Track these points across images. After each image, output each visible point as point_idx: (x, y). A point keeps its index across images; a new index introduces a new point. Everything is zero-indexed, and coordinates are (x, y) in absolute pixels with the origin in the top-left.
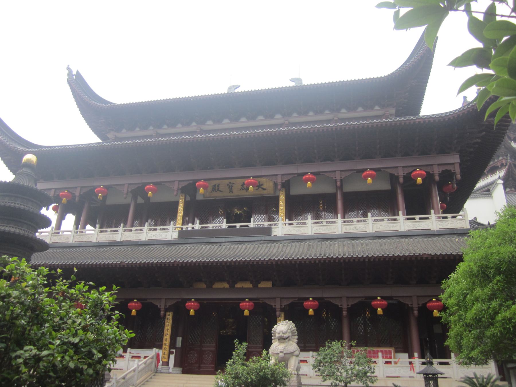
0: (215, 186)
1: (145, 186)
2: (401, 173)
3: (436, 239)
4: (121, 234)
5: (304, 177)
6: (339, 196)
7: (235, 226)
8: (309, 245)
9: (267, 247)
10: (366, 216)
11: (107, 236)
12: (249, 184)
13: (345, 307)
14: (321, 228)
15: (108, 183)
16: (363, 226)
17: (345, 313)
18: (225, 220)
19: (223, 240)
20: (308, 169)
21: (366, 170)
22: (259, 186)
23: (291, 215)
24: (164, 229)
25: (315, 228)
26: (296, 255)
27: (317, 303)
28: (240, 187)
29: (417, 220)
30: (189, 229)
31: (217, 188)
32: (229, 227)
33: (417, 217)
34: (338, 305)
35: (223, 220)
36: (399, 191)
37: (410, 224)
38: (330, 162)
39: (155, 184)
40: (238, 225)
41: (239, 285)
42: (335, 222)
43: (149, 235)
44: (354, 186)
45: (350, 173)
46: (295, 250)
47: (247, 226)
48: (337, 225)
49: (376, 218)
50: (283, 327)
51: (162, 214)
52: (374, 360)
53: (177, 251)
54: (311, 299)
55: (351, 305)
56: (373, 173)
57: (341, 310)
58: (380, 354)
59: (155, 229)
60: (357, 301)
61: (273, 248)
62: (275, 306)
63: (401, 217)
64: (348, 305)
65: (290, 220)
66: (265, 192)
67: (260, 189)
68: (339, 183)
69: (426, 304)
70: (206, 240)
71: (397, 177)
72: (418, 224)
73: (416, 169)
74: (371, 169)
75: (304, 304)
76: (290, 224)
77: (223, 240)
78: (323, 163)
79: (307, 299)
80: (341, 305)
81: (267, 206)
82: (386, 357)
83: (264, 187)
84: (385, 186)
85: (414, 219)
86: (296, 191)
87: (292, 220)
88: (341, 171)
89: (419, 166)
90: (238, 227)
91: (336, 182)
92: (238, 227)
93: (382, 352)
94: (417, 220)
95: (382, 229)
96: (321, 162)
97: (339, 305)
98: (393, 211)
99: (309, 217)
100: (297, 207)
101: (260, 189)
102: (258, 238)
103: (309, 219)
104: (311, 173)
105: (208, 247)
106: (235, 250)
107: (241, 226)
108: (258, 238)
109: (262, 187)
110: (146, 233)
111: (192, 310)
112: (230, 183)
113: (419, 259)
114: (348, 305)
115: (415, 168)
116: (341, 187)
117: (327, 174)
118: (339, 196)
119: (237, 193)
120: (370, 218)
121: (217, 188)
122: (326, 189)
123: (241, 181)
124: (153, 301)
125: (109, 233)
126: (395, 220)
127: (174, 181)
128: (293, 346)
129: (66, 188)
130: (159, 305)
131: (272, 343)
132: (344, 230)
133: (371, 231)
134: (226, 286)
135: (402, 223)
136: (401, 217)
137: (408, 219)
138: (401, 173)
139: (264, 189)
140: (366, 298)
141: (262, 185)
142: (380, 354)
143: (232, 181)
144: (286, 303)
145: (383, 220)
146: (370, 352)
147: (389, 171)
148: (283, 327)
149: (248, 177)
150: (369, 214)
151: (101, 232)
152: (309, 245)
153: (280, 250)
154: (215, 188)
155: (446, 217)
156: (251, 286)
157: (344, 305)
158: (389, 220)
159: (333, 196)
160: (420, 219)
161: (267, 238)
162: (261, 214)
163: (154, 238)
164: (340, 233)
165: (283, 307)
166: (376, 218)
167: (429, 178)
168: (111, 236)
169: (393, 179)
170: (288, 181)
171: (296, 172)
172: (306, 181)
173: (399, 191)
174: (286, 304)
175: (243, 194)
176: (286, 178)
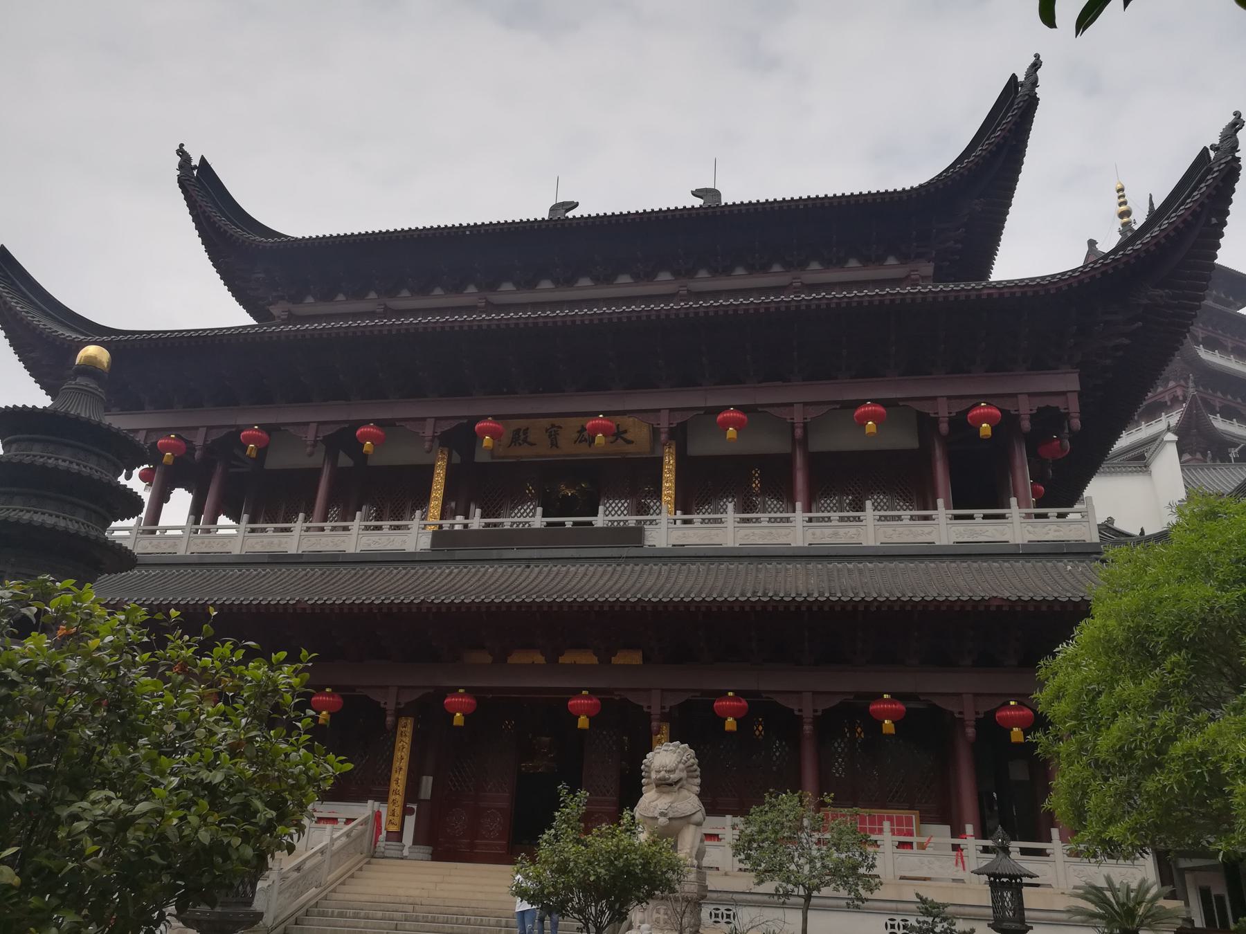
0: (517, 431)
2: (944, 412)
4: (298, 538)
5: (720, 417)
6: (799, 461)
7: (563, 524)
9: (633, 571)
10: (861, 508)
11: (266, 540)
13: (808, 714)
14: (756, 531)
15: (270, 418)
16: (853, 531)
17: (807, 728)
18: (539, 510)
19: (535, 553)
20: (729, 399)
22: (618, 434)
23: (685, 503)
24: (398, 528)
25: (742, 532)
26: (700, 592)
27: (744, 703)
29: (979, 520)
30: (457, 527)
31: (522, 437)
32: (549, 524)
33: (979, 513)
34: (792, 710)
35: (535, 508)
36: (938, 453)
37: (961, 528)
38: (780, 383)
39: (379, 423)
40: (569, 521)
41: (566, 659)
42: (788, 520)
43: (364, 539)
44: (836, 440)
45: (825, 409)
47: (590, 523)
48: (797, 529)
49: (883, 513)
50: (666, 757)
51: (396, 494)
52: (873, 837)
54: (730, 694)
55: (823, 711)
56: (880, 409)
57: (799, 721)
58: (886, 825)
59: (379, 528)
60: (836, 701)
61: (646, 574)
62: (649, 707)
63: (942, 512)
64: (815, 711)
66: (630, 448)
67: (620, 441)
68: (799, 432)
70: (494, 554)
71: (936, 421)
72: (981, 530)
73: (978, 404)
74: (875, 402)
76: (685, 522)
77: (535, 553)
78: (764, 384)
79: (722, 694)
80: (800, 710)
81: (637, 483)
82: (900, 833)
83: (628, 436)
84: (905, 440)
85: (971, 517)
86: (701, 446)
88: (805, 404)
89: (984, 397)
90: (569, 525)
92: (569, 525)
93: (890, 819)
97: (796, 708)
98: (922, 499)
99: (731, 506)
101: (620, 441)
104: (737, 408)
105: (500, 570)
107: (575, 524)
109: (625, 436)
110: (358, 537)
112: (553, 426)
113: (982, 608)
114: (815, 711)
116: (804, 441)
117: (771, 410)
118: (799, 461)
119: (568, 448)
120: (870, 512)
121: (522, 437)
122: (770, 444)
123: (575, 423)
125: (270, 533)
126: (926, 518)
127: (424, 419)
128: (688, 801)
129: (171, 430)
133: (871, 543)
134: (539, 659)
135: (944, 528)
136: (942, 512)
137: (957, 517)
138: (944, 412)
141: (625, 432)
142: (886, 825)
143: (557, 421)
144: (672, 701)
145: (899, 518)
146: (863, 821)
147: (917, 406)
148: (666, 757)
150: (868, 504)
151: (253, 531)
154: (519, 437)
155: (1045, 516)
156: (594, 660)
157: (808, 710)
158: (912, 518)
160: (985, 517)
164: (800, 544)
166: (883, 513)
167: (1006, 425)
168: (276, 540)
169: (926, 425)
170: (683, 427)
172: (725, 425)
173: (938, 453)
174: (673, 704)
176: (678, 418)
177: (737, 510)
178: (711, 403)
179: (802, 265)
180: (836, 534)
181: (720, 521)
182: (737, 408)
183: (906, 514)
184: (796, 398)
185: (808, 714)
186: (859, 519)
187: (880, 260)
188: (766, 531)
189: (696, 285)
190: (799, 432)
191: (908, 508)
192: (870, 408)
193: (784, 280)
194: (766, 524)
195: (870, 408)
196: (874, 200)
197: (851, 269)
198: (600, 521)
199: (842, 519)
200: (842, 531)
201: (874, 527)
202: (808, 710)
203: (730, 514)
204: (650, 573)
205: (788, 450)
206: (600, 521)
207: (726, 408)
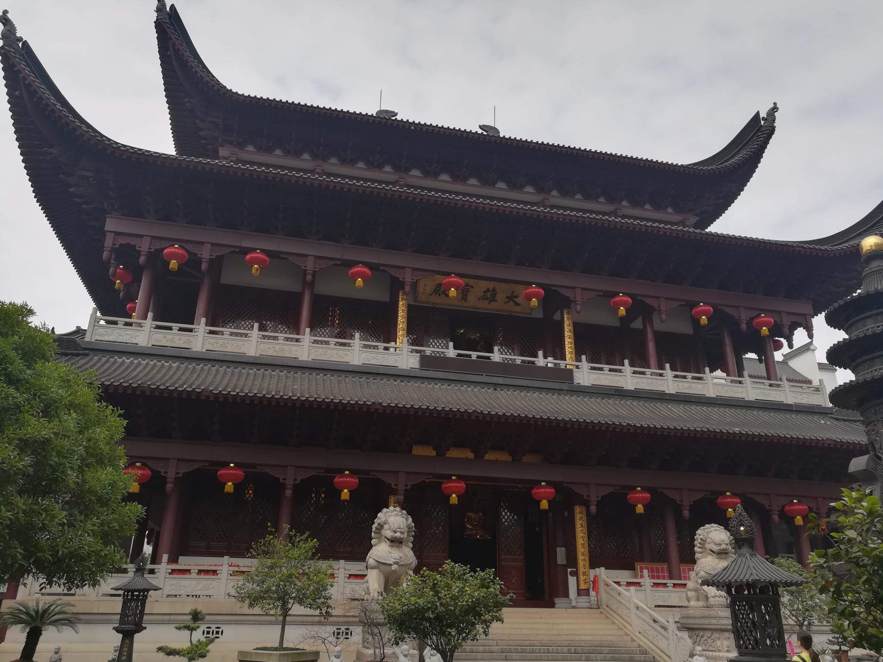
1: (247, 254)
2: (144, 246)
3: (350, 379)
4: (200, 338)
5: (248, 257)
6: (650, 335)
7: (470, 356)
8: (248, 374)
11: (277, 347)
12: (449, 286)
13: (290, 482)
15: (272, 246)
16: (700, 386)
18: (451, 344)
19: (501, 381)
20: (259, 244)
21: (253, 250)
22: (512, 298)
23: (216, 320)
25: (364, 355)
26: (182, 385)
27: (462, 485)
28: (481, 294)
29: (175, 331)
30: (550, 365)
32: (459, 355)
33: (176, 326)
35: (447, 343)
36: (727, 341)
40: (474, 355)
42: (246, 335)
43: (263, 346)
44: (331, 287)
45: (331, 263)
46: (206, 377)
47: (489, 358)
48: (306, 347)
52: (152, 567)
53: (103, 365)
54: (232, 465)
58: (645, 572)
60: (196, 466)
61: (252, 378)
62: (284, 479)
63: (201, 326)
65: (555, 359)
66: (517, 309)
67: (511, 303)
68: (309, 277)
69: (784, 507)
71: (199, 262)
72: (173, 338)
74: (539, 285)
75: (443, 486)
76: (386, 349)
80: (284, 479)
81: (539, 334)
83: (518, 300)
85: (170, 328)
86: (229, 277)
87: (276, 332)
88: (153, 237)
91: (305, 276)
94: (175, 331)
95: (271, 353)
96: (319, 240)
99: (357, 335)
100: (600, 345)
101: (511, 303)
102: (441, 375)
103: (357, 341)
104: (262, 251)
105: (104, 359)
106: (123, 368)
107: (478, 357)
108: (441, 375)
109: (516, 300)
110: (357, 352)
111: (454, 495)
112: (467, 285)
113: (554, 424)
115: (756, 313)
116: (312, 285)
118: (650, 335)
119: (500, 305)
120: (357, 341)
123: (484, 285)
124: (270, 471)
127: (202, 243)
129: (176, 241)
130: (393, 484)
131: (371, 547)
132: (313, 356)
135: (669, 382)
136: (201, 326)
137: (158, 327)
138: (144, 246)
139: (517, 304)
140: (213, 463)
141: (517, 297)
142: (645, 572)
143: (471, 282)
147: (391, 271)
149: (448, 274)
152: (248, 374)
153: (219, 377)
155: (115, 323)
159: (295, 299)
160: (181, 329)
161: (565, 387)
162: (324, 327)
163: (325, 358)
164: (305, 358)
165: (298, 482)
167: (191, 263)
168: (286, 348)
170: (220, 259)
171: (339, 257)
173: (727, 341)
174: (303, 478)
175: (485, 306)
176: (218, 252)
177: (155, 319)
178: (611, 288)
179: (325, 158)
180: (690, 387)
181: (348, 345)
182: (262, 251)
183: (281, 336)
184: (311, 252)
185: (290, 482)
186: (297, 340)
187: (380, 167)
188: (650, 381)
189: (329, 168)
190: (309, 277)
191: (286, 333)
192: (534, 288)
193: (393, 177)
194: (282, 341)
195: (534, 288)
196: (276, 105)
197: (647, 210)
198: (497, 356)
199: (287, 339)
200: (694, 385)
201: (251, 342)
202: (290, 478)
203: (627, 368)
204: (208, 373)
205: (300, 290)
206: (497, 356)
207: (253, 250)
